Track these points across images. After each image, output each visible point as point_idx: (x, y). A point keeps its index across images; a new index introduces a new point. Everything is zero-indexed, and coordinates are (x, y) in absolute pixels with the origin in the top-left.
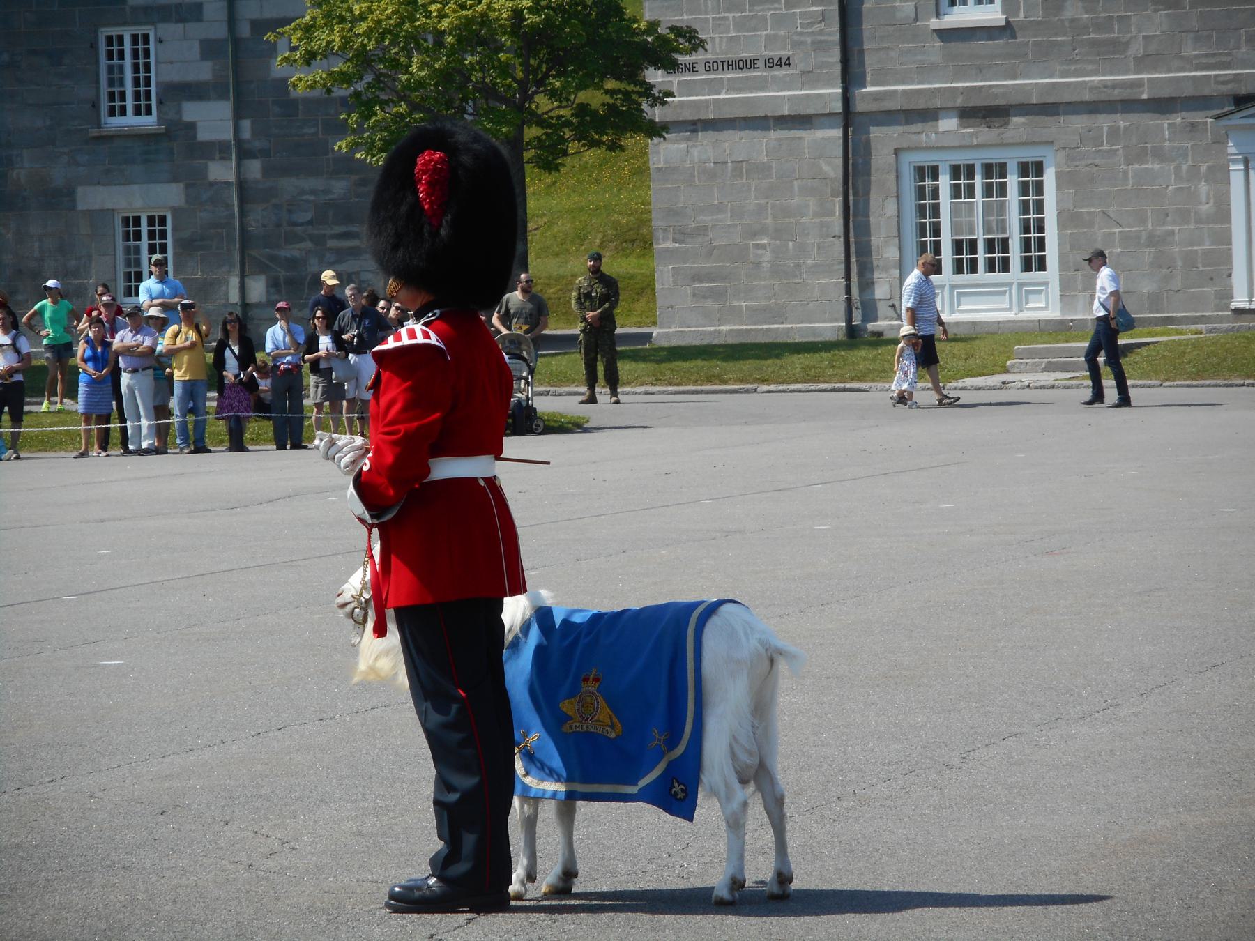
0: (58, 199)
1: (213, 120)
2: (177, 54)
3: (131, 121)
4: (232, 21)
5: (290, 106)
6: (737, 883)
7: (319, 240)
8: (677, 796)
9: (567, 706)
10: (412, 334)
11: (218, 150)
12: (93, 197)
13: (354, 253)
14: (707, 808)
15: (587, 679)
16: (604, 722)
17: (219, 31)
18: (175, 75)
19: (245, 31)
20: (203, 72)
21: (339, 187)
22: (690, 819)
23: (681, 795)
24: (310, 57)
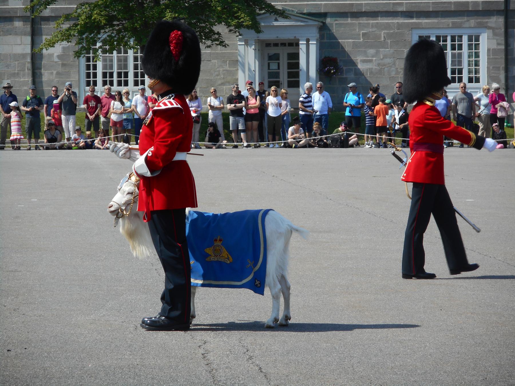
6: (276, 320)
8: (258, 287)
9: (209, 251)
10: (165, 104)
14: (267, 290)
15: (216, 240)
16: (226, 257)
22: (263, 294)
23: (259, 285)
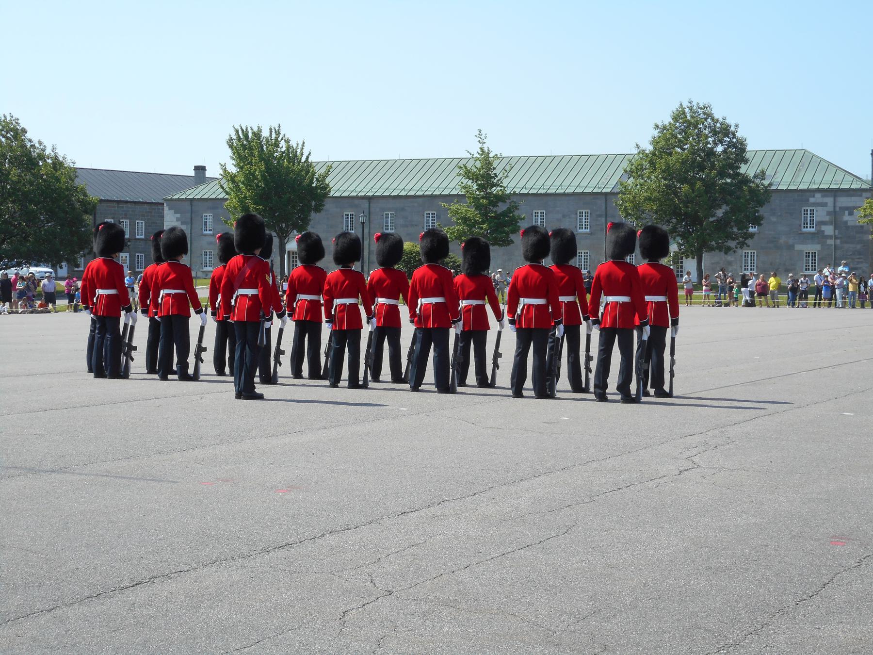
0: (791, 247)
1: (829, 230)
2: (820, 214)
3: (809, 230)
4: (834, 207)
5: (847, 227)
7: (853, 259)
11: (830, 237)
12: (798, 247)
13: (861, 262)
17: (832, 209)
18: (820, 219)
19: (837, 209)
20: (827, 219)
21: (859, 247)
24: (865, 216)
